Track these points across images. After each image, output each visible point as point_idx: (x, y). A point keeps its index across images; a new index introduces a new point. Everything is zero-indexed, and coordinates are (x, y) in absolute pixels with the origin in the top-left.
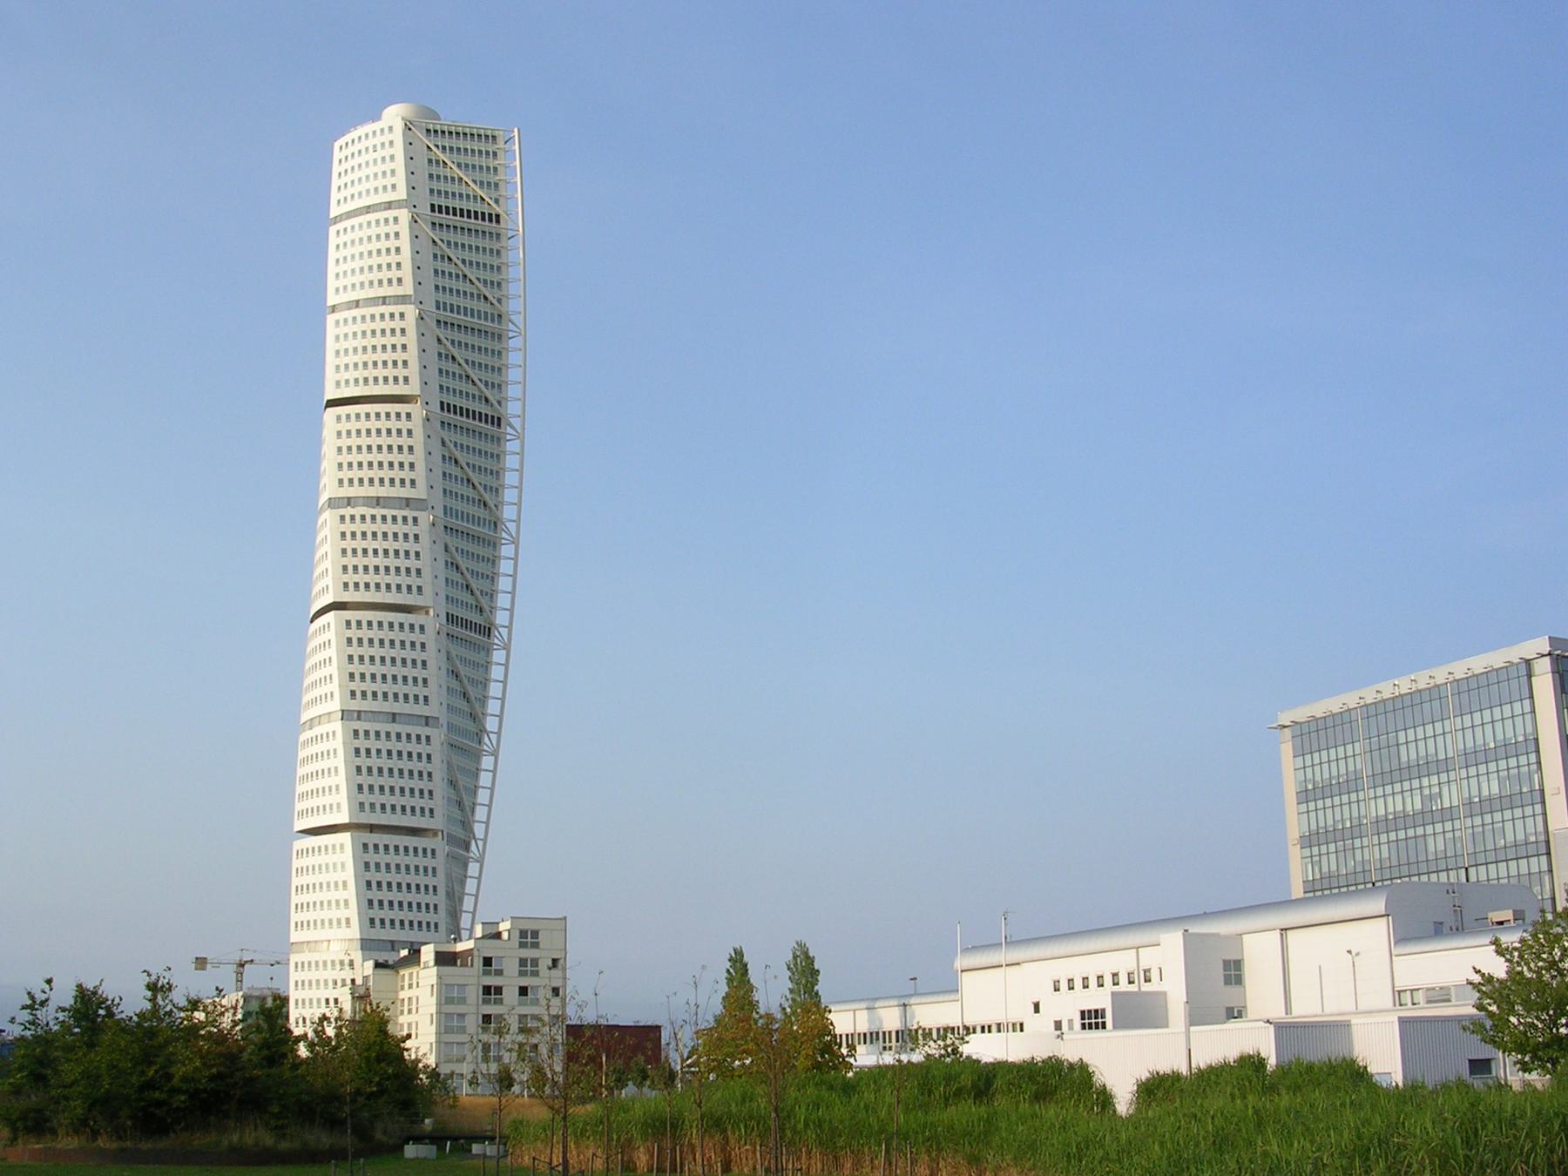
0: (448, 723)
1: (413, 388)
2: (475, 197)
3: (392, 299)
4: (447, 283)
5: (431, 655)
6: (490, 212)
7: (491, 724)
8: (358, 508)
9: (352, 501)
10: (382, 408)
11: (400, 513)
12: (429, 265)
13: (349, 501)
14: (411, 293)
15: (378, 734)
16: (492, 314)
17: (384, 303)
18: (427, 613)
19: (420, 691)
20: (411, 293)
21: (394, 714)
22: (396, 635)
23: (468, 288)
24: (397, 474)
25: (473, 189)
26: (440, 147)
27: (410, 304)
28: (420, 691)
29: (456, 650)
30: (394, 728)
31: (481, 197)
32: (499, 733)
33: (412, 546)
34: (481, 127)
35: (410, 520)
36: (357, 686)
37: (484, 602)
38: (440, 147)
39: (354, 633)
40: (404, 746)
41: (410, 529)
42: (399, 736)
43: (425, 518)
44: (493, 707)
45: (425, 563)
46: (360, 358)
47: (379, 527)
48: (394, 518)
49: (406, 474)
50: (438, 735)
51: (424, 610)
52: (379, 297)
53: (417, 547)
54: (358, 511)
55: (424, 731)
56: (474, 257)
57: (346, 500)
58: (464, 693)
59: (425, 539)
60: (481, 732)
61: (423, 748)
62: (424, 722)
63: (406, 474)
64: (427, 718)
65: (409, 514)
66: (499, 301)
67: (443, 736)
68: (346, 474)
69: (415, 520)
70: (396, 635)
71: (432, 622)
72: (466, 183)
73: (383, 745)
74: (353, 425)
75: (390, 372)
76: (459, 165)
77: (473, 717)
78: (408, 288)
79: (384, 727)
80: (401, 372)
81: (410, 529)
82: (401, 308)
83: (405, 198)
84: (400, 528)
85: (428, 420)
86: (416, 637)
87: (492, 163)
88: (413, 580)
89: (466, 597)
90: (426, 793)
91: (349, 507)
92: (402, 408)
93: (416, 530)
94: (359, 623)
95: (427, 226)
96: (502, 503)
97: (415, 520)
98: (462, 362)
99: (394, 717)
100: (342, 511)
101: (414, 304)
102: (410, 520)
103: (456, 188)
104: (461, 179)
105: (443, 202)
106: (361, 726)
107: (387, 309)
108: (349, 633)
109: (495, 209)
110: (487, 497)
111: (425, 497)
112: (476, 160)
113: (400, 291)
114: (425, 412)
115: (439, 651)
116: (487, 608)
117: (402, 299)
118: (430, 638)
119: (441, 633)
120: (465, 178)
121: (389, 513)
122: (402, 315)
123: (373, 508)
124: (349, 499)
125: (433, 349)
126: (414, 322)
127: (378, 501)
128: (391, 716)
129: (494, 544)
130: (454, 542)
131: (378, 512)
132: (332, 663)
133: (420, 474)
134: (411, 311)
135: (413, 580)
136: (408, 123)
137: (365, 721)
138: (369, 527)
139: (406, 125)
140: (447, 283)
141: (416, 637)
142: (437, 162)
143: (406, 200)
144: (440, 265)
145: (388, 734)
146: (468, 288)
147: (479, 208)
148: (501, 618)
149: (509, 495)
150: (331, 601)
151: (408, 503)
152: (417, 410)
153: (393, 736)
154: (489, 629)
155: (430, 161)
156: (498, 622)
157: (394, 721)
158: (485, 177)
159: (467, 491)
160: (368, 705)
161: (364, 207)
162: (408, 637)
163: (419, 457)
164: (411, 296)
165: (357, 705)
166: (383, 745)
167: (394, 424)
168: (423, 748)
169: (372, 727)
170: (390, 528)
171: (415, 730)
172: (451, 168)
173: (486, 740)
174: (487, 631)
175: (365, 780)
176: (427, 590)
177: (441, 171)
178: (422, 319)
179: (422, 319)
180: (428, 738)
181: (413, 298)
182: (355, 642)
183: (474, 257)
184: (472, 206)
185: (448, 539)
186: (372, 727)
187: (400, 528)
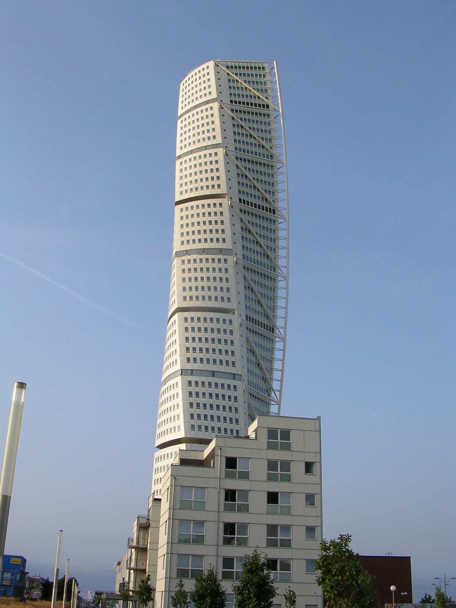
0: (248, 380)
1: (223, 190)
2: (255, 97)
3: (210, 146)
4: (241, 138)
5: (236, 337)
6: (263, 103)
7: (276, 385)
8: (193, 255)
9: (189, 252)
10: (205, 202)
11: (216, 257)
12: (230, 130)
13: (187, 252)
14: (221, 142)
15: (203, 383)
16: (268, 156)
17: (206, 149)
18: (234, 314)
19: (229, 358)
20: (221, 142)
21: (213, 372)
22: (215, 325)
23: (253, 141)
24: (214, 236)
25: (253, 92)
26: (234, 73)
27: (220, 148)
28: (229, 358)
29: (252, 337)
30: (214, 380)
31: (258, 96)
32: (280, 391)
33: (224, 275)
34: (256, 62)
35: (222, 261)
36: (191, 355)
37: (270, 313)
38: (234, 73)
39: (189, 325)
40: (220, 391)
41: (223, 265)
42: (216, 385)
43: (232, 259)
44: (276, 375)
45: (232, 284)
46: (193, 178)
47: (204, 265)
48: (213, 260)
49: (220, 236)
50: (241, 385)
51: (232, 313)
52: (203, 147)
53: (227, 275)
54: (192, 257)
55: (233, 383)
56: (255, 126)
57: (185, 252)
58: (258, 364)
59: (231, 271)
60: (269, 390)
61: (232, 393)
62: (232, 377)
63: (220, 236)
64: (234, 374)
65: (222, 257)
66: (271, 148)
67: (244, 386)
68: (185, 238)
69: (226, 260)
70: (215, 325)
71: (237, 319)
72: (249, 89)
73: (207, 390)
74: (190, 212)
75: (210, 183)
76: (245, 82)
77: (265, 379)
78: (219, 141)
79: (207, 380)
80: (216, 182)
81: (223, 265)
82: (215, 150)
83: (216, 97)
84: (217, 265)
85: (232, 207)
86: (227, 326)
87: (263, 80)
88: (225, 294)
89: (258, 308)
90: (234, 421)
91: (187, 256)
92: (217, 201)
93: (226, 266)
94: (192, 319)
95: (230, 111)
96: (278, 256)
97: (226, 260)
98: (251, 179)
99: (213, 374)
100: (183, 258)
101: (222, 147)
102: (222, 261)
103: (244, 92)
104: (246, 88)
105: (237, 99)
106: (193, 378)
107: (207, 152)
108: (186, 325)
109: (266, 102)
110: (269, 252)
111: (232, 248)
112: (254, 78)
113: (214, 142)
114: (230, 202)
115: (242, 336)
116: (272, 317)
117: (216, 146)
118: (235, 327)
119: (242, 325)
120: (249, 87)
121: (210, 257)
122: (216, 154)
123: (202, 255)
124: (187, 251)
125: (234, 171)
126: (223, 156)
127: (203, 251)
128: (211, 372)
129: (274, 280)
130: (249, 275)
131: (204, 257)
132: (177, 343)
133: (228, 235)
134: (221, 151)
135: (225, 294)
136: (216, 63)
137: (196, 376)
138: (198, 265)
139: (215, 63)
140: (241, 138)
141: (227, 326)
142: (233, 81)
143: (217, 98)
144: (236, 130)
145: (210, 384)
146: (253, 141)
147: (257, 102)
148: (280, 323)
149: (281, 253)
150: (177, 307)
151: (221, 251)
152: (226, 202)
153: (213, 385)
154: (273, 329)
155: (229, 80)
156: (277, 325)
157: (213, 376)
158: (259, 87)
159: (257, 248)
160: (197, 366)
161: (195, 106)
162: (222, 326)
163: (227, 226)
164: (220, 144)
165: (191, 366)
166: (207, 390)
167: (212, 210)
168: (232, 393)
169: (200, 379)
170: (210, 265)
171: (226, 382)
172: (241, 83)
173: (273, 395)
174: (272, 329)
175: (195, 411)
176: (234, 300)
177: (235, 85)
178: (227, 155)
179: (227, 155)
180: (235, 387)
181: (222, 144)
182: (190, 329)
183: (255, 126)
184: (253, 101)
185: (246, 273)
186: (200, 379)
187: (217, 265)
